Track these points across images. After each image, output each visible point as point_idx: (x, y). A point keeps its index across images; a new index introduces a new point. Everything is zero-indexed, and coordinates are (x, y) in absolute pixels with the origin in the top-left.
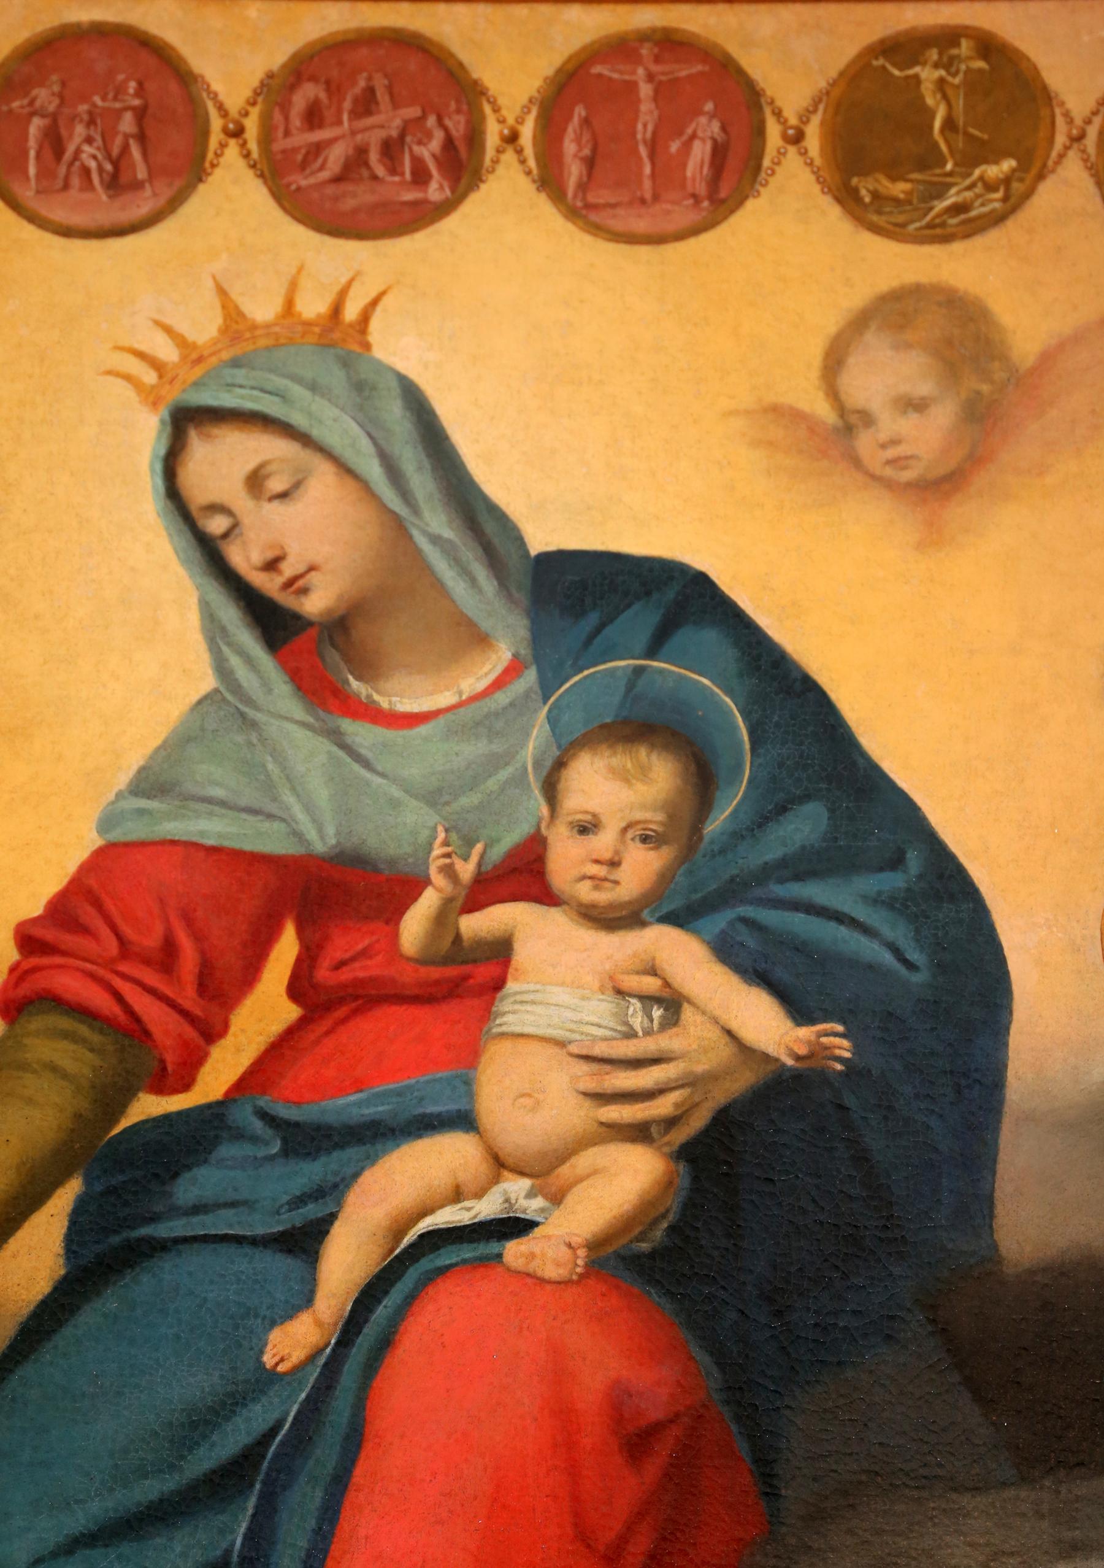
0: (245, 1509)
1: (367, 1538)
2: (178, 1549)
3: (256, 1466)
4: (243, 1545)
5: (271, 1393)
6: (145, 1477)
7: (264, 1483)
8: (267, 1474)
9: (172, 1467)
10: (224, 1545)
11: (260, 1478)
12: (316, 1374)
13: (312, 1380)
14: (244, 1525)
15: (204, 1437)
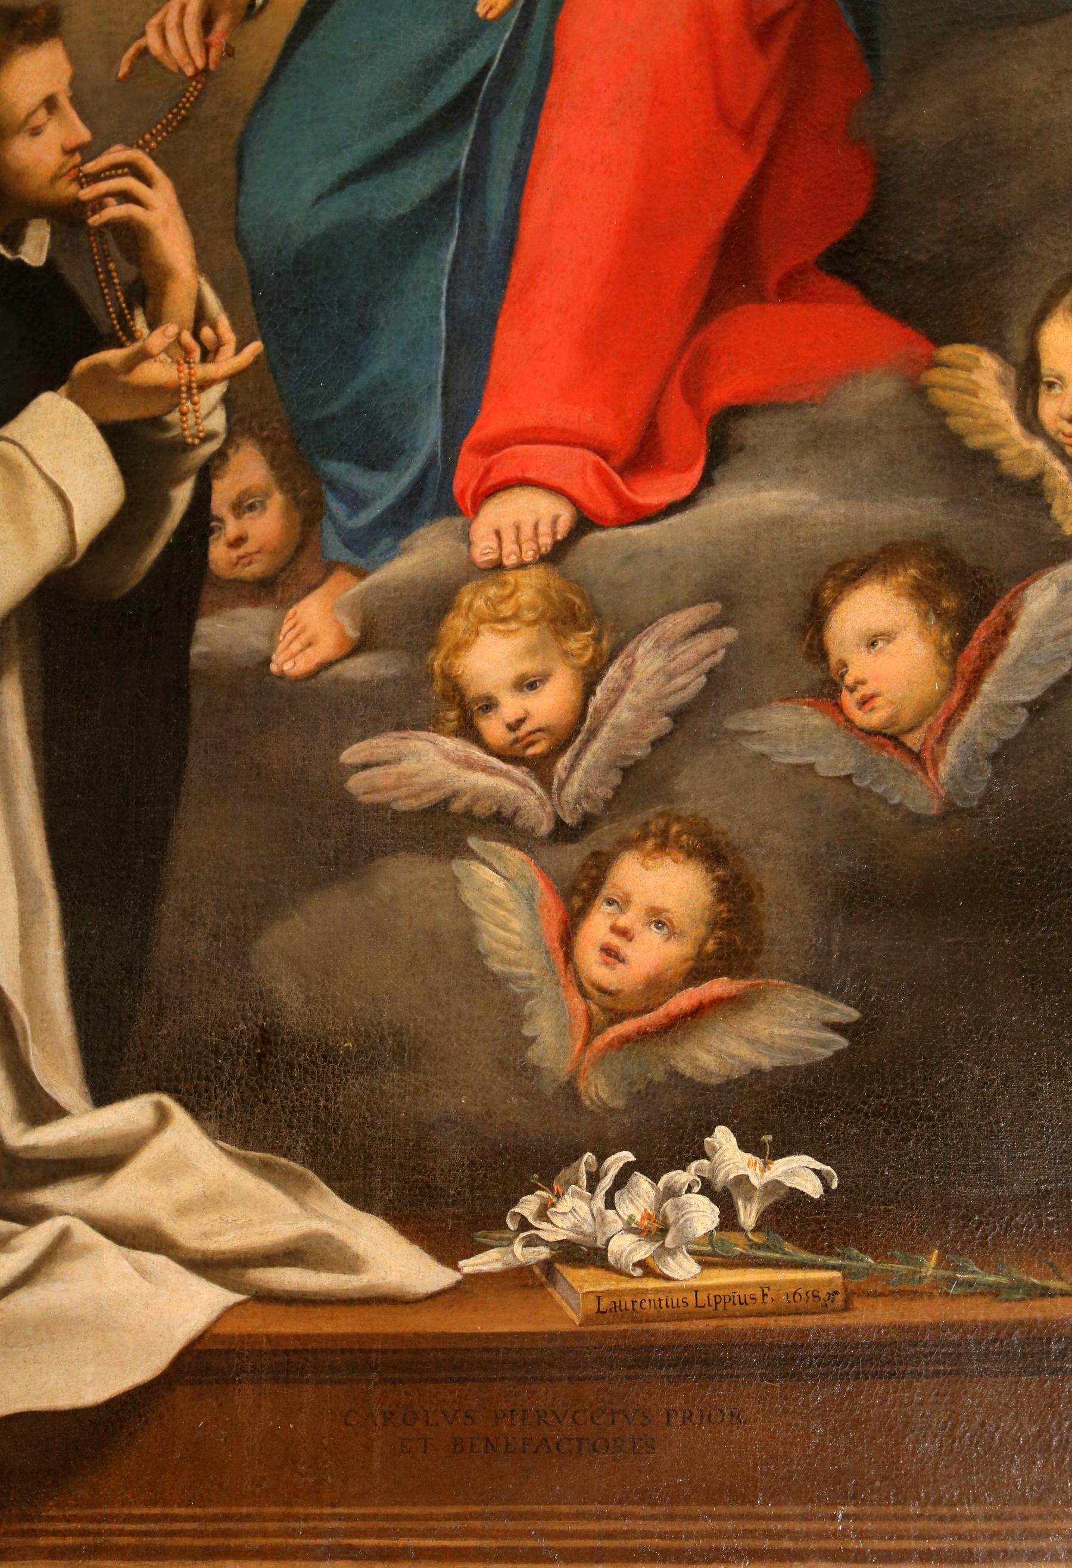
0: (467, 136)
1: (558, 146)
2: (419, 175)
3: (473, 100)
4: (467, 165)
5: (484, 37)
6: (394, 120)
7: (481, 112)
8: (483, 104)
9: (413, 109)
10: (453, 167)
11: (477, 108)
12: (516, 16)
13: (513, 21)
14: (467, 148)
15: (435, 81)
